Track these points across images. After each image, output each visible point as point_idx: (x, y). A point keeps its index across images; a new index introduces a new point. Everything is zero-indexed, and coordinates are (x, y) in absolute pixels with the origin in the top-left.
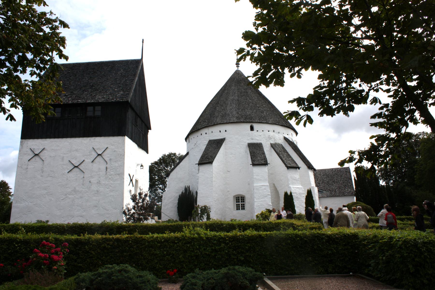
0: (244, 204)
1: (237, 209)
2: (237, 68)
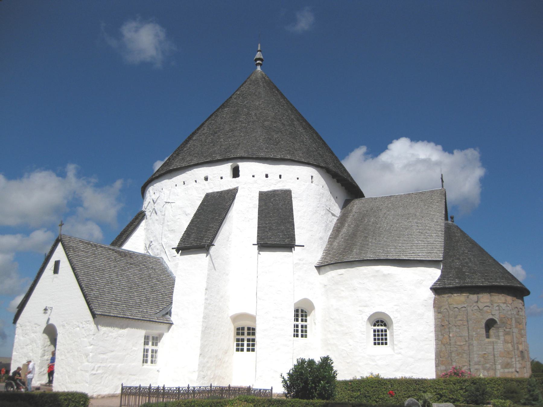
0: (253, 340)
1: (238, 350)
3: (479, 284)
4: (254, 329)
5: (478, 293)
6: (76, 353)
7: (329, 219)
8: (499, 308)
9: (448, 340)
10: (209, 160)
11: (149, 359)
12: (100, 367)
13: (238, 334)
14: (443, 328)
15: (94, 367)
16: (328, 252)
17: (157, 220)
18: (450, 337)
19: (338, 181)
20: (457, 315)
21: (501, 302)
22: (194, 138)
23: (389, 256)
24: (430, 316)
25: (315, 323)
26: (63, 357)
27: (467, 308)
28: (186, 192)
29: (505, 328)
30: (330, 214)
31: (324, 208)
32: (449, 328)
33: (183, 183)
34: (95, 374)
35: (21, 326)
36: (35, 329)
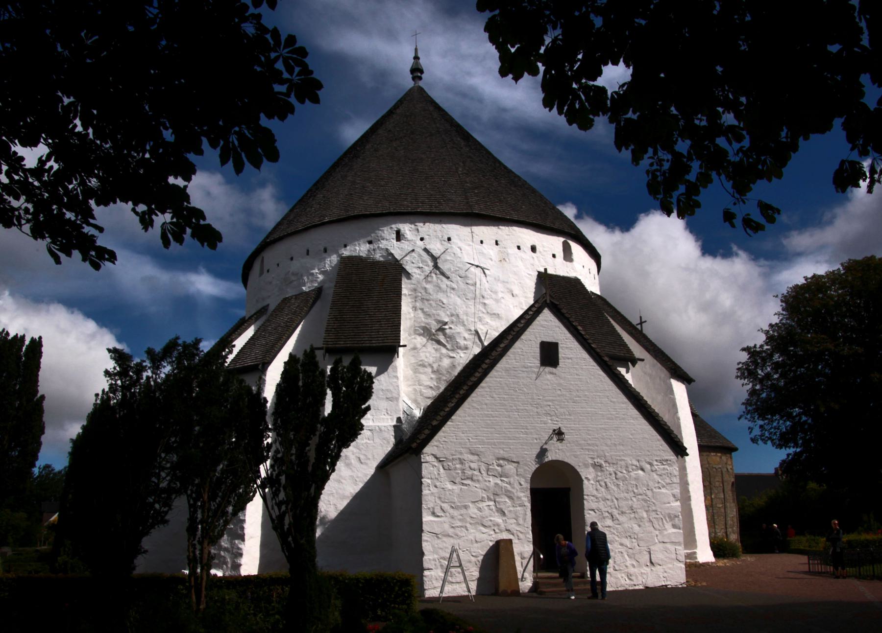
9: (710, 502)
18: (711, 498)
36: (499, 469)
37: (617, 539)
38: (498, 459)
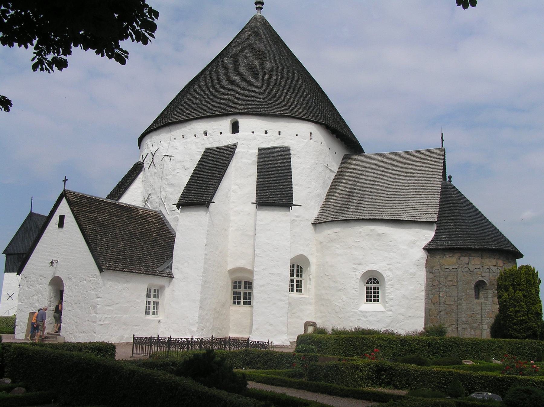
0: (250, 294)
1: (234, 303)
2: (257, 11)
3: (471, 247)
4: (251, 283)
5: (470, 256)
6: (83, 305)
7: (327, 176)
8: (489, 270)
10: (209, 115)
11: (151, 310)
12: (106, 318)
13: (235, 287)
14: (434, 287)
15: (101, 318)
16: (325, 208)
17: (155, 173)
19: (337, 137)
20: (448, 276)
21: (492, 264)
22: (193, 90)
23: (384, 216)
24: (422, 275)
25: (310, 279)
26: (70, 308)
27: (457, 269)
28: (186, 146)
29: (494, 290)
30: (328, 170)
31: (322, 165)
32: (439, 288)
33: (182, 137)
34: (102, 325)
35: (26, 278)
36: (40, 280)
37: (72, 317)
38: (41, 276)
